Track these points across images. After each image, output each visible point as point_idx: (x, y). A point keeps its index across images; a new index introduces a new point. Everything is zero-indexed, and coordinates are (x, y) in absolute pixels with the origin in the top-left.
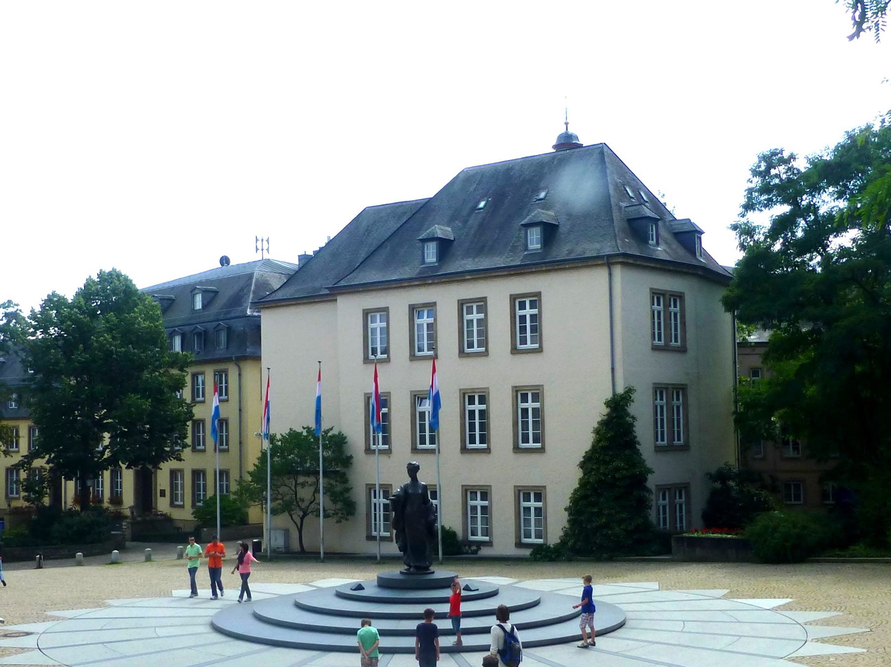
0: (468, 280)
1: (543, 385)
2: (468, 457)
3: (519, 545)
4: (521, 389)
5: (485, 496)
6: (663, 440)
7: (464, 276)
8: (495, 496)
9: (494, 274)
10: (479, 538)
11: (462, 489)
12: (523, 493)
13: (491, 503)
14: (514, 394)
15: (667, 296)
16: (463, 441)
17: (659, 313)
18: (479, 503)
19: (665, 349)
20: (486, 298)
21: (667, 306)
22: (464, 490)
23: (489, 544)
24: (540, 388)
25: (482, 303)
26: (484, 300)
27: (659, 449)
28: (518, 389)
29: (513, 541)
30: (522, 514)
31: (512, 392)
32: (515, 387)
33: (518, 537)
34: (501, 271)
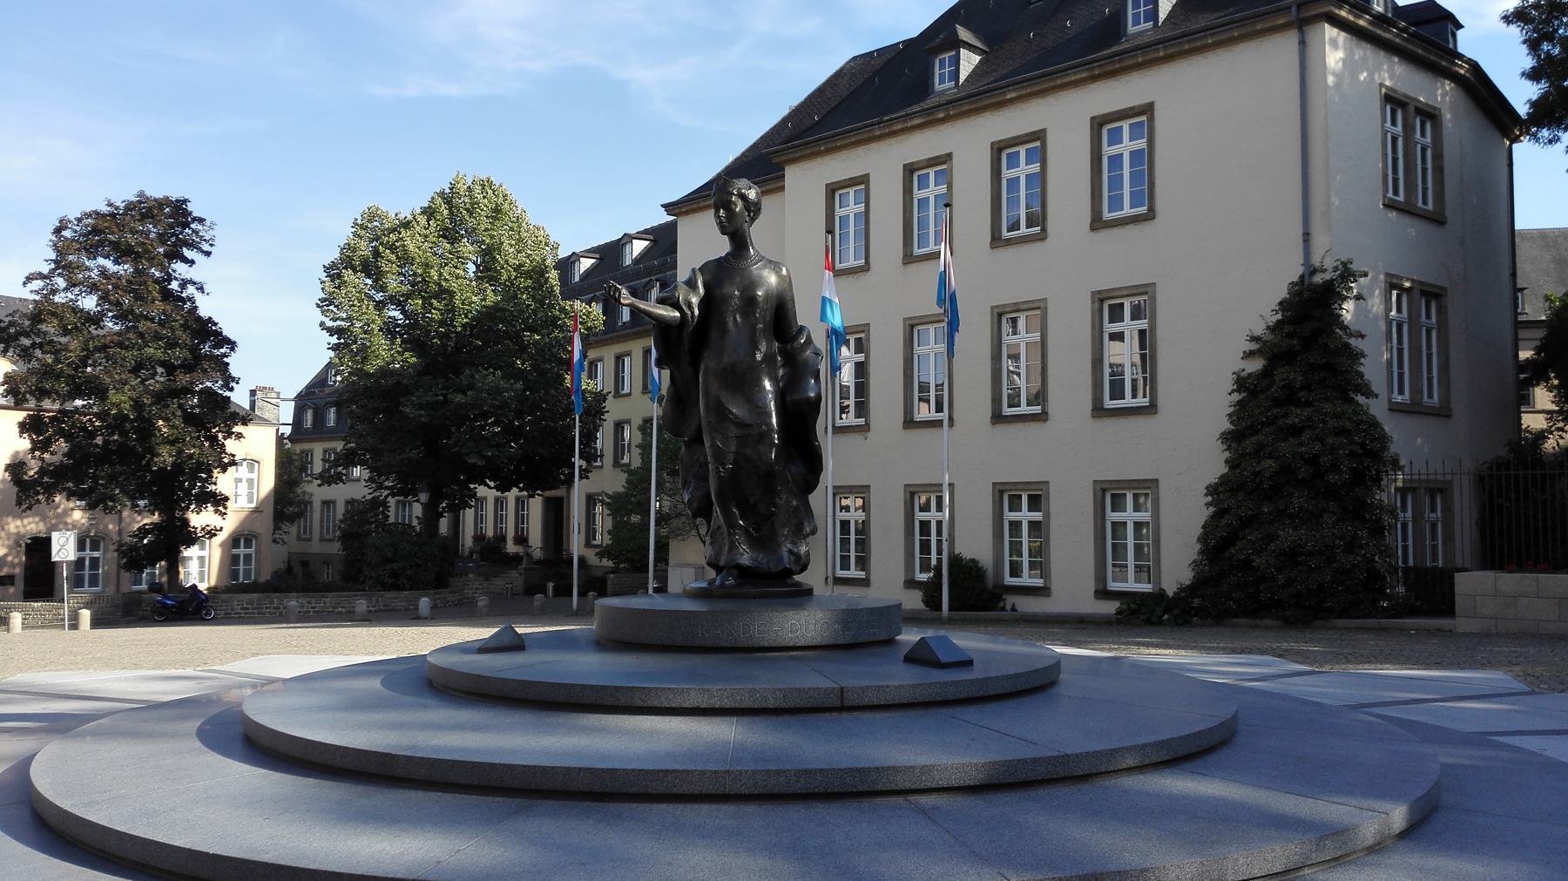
0: (1011, 102)
1: (1154, 284)
2: (1003, 429)
3: (1103, 593)
4: (1111, 295)
5: (1035, 503)
6: (1401, 392)
7: (1004, 93)
8: (1056, 502)
9: (1059, 82)
10: (1027, 579)
11: (993, 489)
12: (1109, 494)
13: (1047, 516)
14: (1097, 305)
15: (1411, 109)
16: (996, 401)
17: (1394, 140)
18: (1025, 515)
19: (1406, 210)
20: (1044, 131)
21: (1408, 128)
22: (997, 491)
23: (1043, 591)
24: (1149, 289)
25: (1038, 144)
26: (1039, 136)
27: (1395, 408)
28: (1102, 296)
29: (1091, 586)
30: (1107, 539)
31: (1093, 302)
32: (1099, 292)
33: (1101, 577)
34: (1075, 73)
